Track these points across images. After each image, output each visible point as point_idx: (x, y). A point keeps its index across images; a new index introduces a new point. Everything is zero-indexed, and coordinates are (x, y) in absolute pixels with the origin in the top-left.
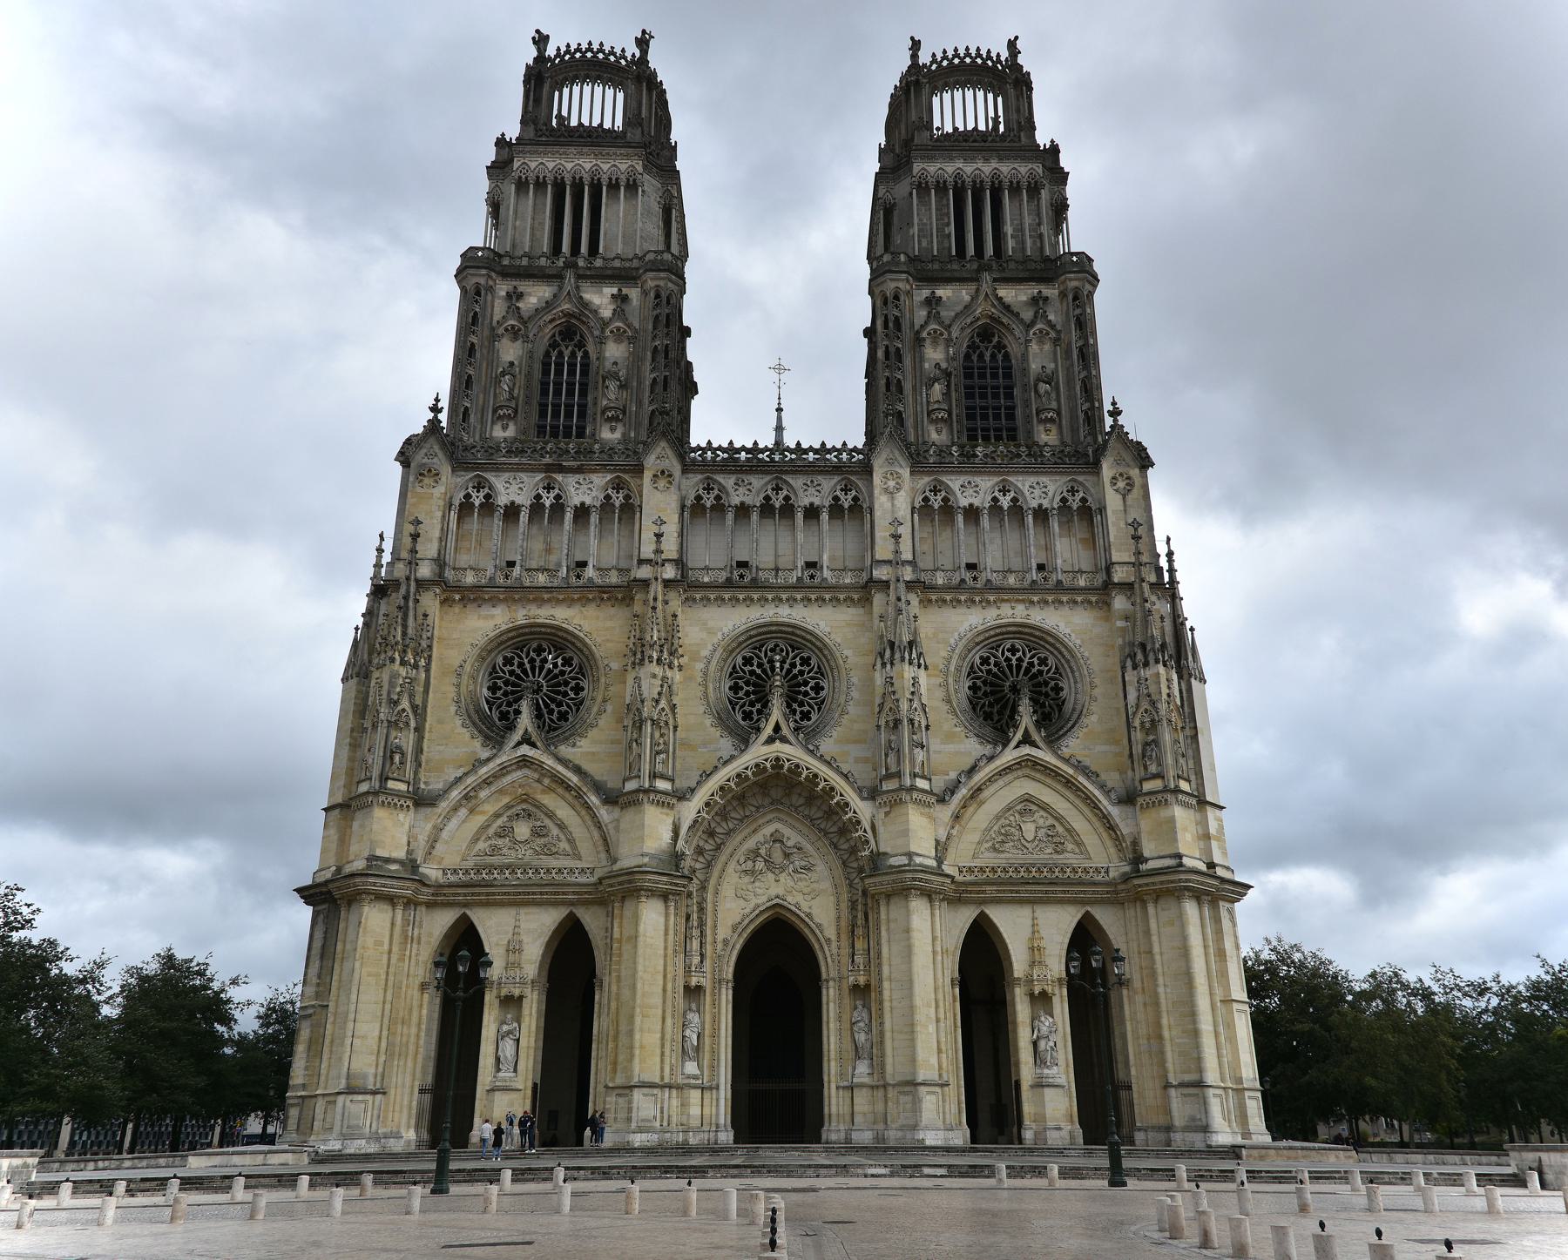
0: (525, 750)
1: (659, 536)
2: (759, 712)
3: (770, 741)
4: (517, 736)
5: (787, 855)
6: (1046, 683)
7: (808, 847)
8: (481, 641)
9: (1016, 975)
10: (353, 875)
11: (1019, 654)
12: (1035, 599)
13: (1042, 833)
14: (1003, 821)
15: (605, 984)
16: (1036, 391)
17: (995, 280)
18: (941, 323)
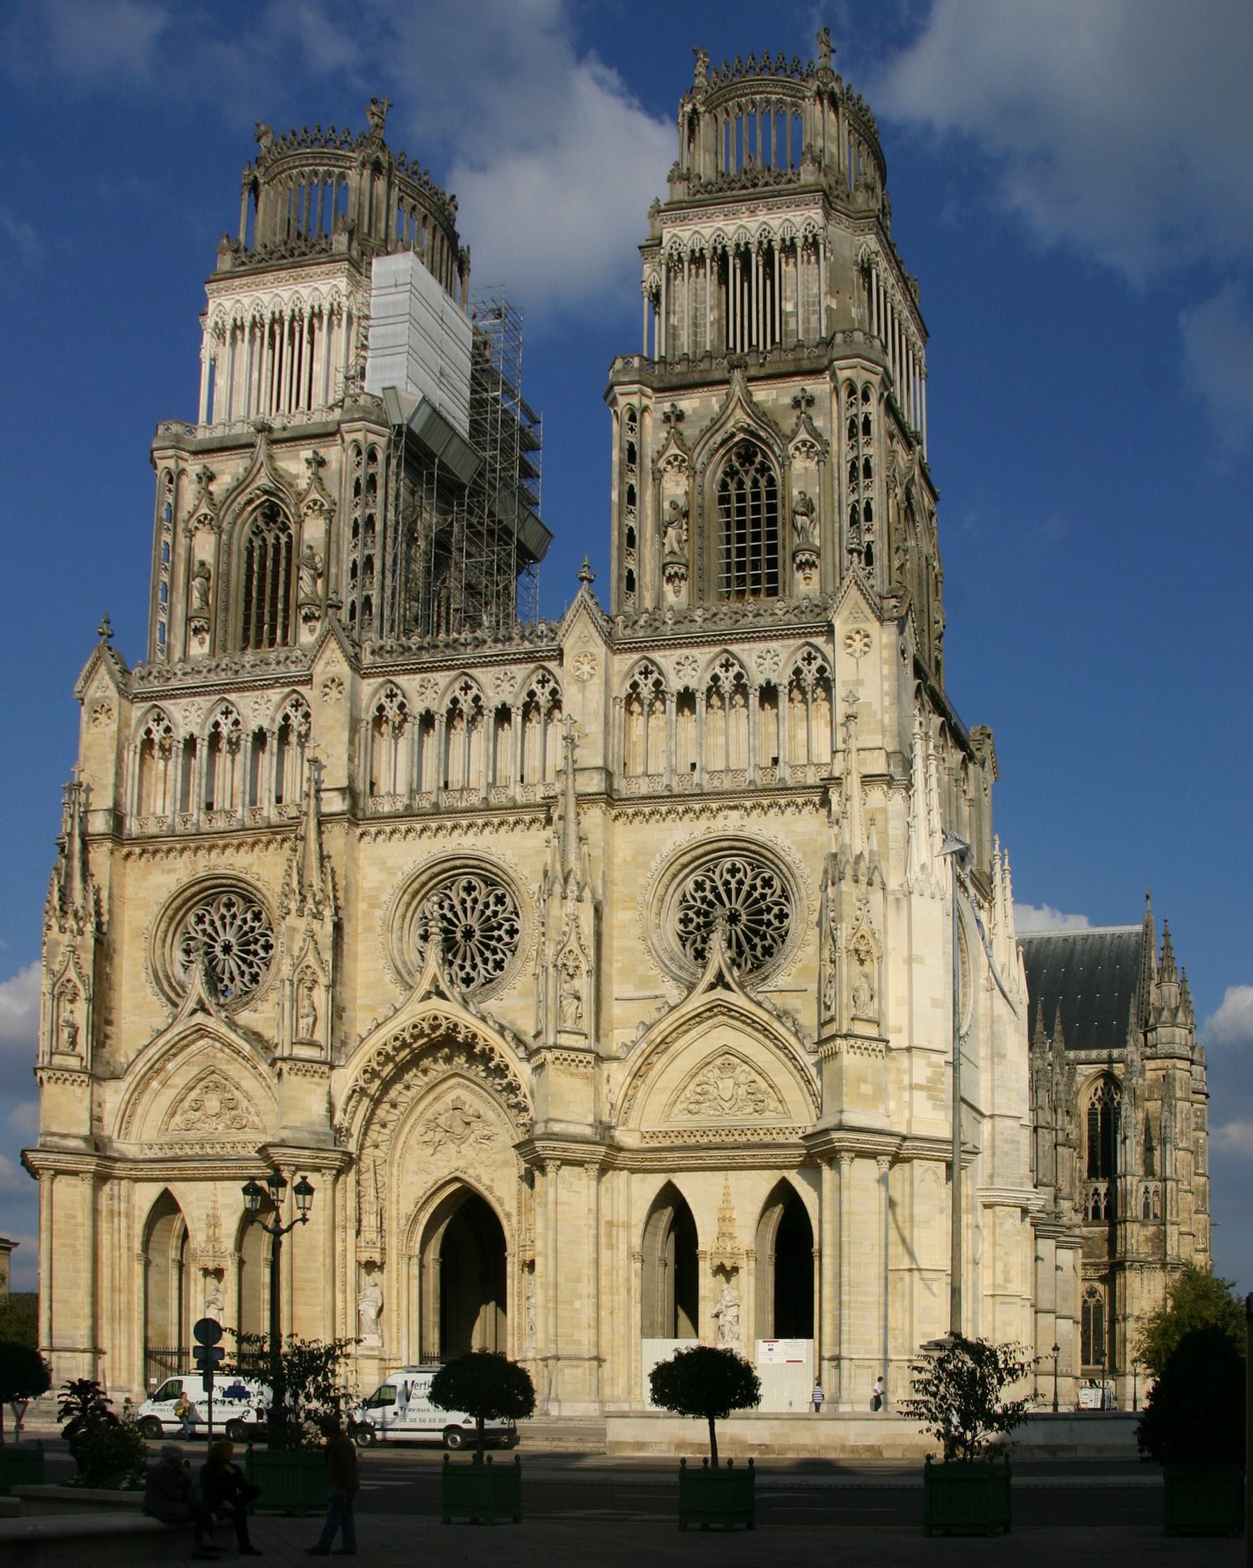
0: (200, 1017)
6: (769, 910)
7: (490, 1115)
8: (164, 897)
9: (701, 1248)
11: (739, 876)
12: (748, 804)
13: (742, 1091)
14: (699, 1078)
16: (794, 526)
17: (751, 379)
18: (681, 444)
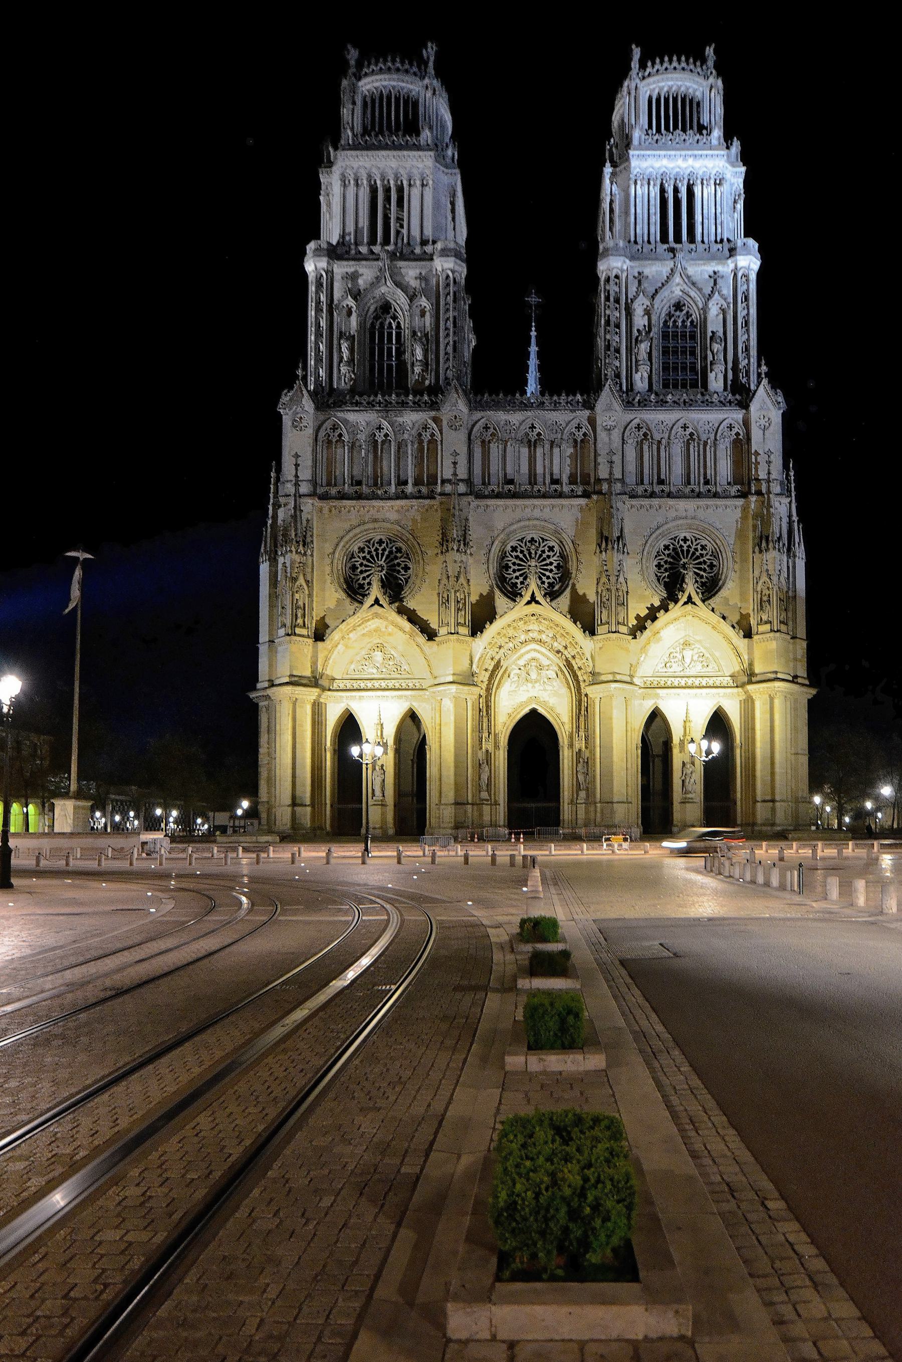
1: (455, 463)
2: (522, 583)
3: (529, 603)
4: (370, 600)
5: (539, 674)
10: (280, 685)
15: (433, 749)
